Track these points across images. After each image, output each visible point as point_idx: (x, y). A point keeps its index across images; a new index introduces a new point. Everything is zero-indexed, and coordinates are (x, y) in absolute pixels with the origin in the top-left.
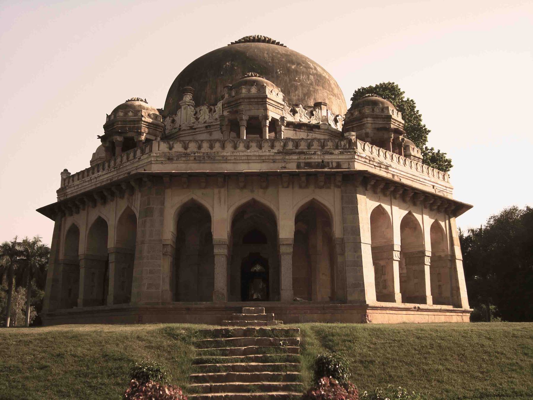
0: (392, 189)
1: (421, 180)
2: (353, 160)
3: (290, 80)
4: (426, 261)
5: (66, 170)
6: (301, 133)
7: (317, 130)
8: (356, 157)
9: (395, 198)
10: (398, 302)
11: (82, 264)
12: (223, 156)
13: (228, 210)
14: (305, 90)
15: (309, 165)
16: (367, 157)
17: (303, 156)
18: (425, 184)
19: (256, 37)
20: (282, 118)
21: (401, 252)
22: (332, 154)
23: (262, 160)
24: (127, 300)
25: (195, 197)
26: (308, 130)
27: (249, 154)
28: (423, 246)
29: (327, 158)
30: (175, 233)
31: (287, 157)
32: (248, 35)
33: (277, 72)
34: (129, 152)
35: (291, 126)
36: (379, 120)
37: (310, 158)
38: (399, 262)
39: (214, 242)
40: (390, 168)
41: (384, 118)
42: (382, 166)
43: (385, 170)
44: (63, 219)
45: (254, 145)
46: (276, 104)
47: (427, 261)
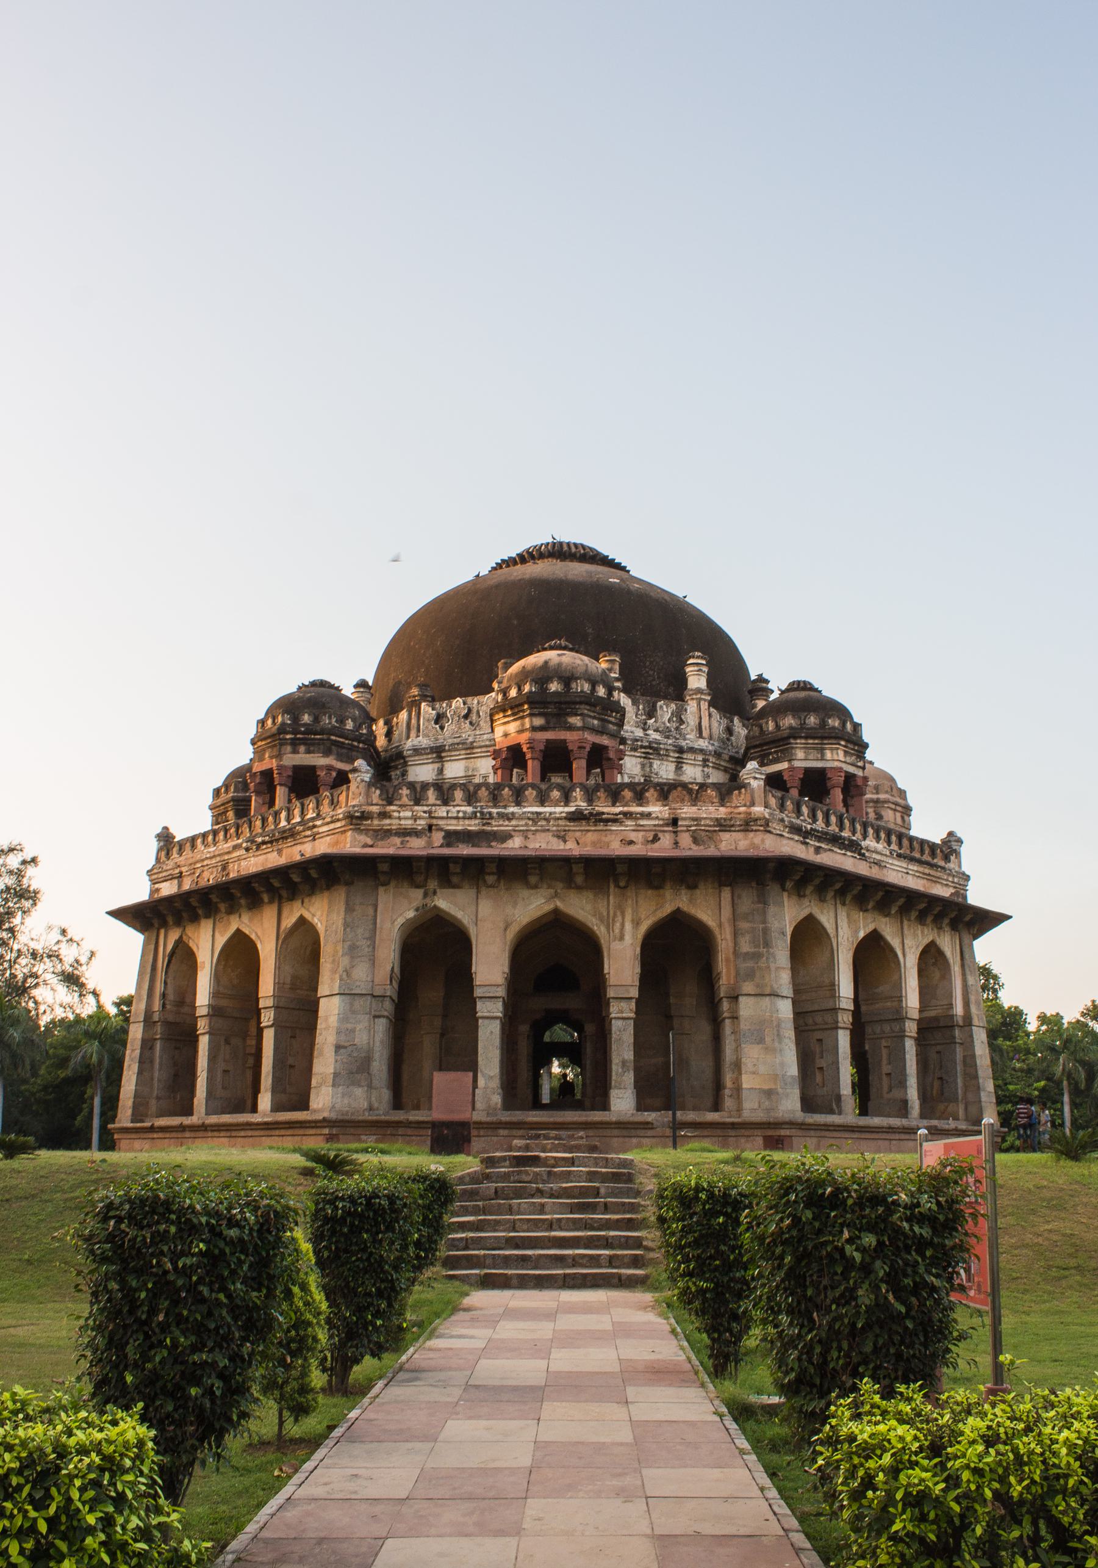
0: (838, 886)
4: (907, 1029)
5: (166, 828)
9: (844, 904)
10: (849, 1115)
11: (202, 1025)
13: (505, 930)
19: (565, 548)
21: (856, 1013)
24: (304, 1105)
28: (900, 999)
30: (397, 970)
34: (307, 801)
38: (851, 1031)
39: (478, 992)
44: (162, 931)
45: (556, 794)
47: (911, 1028)
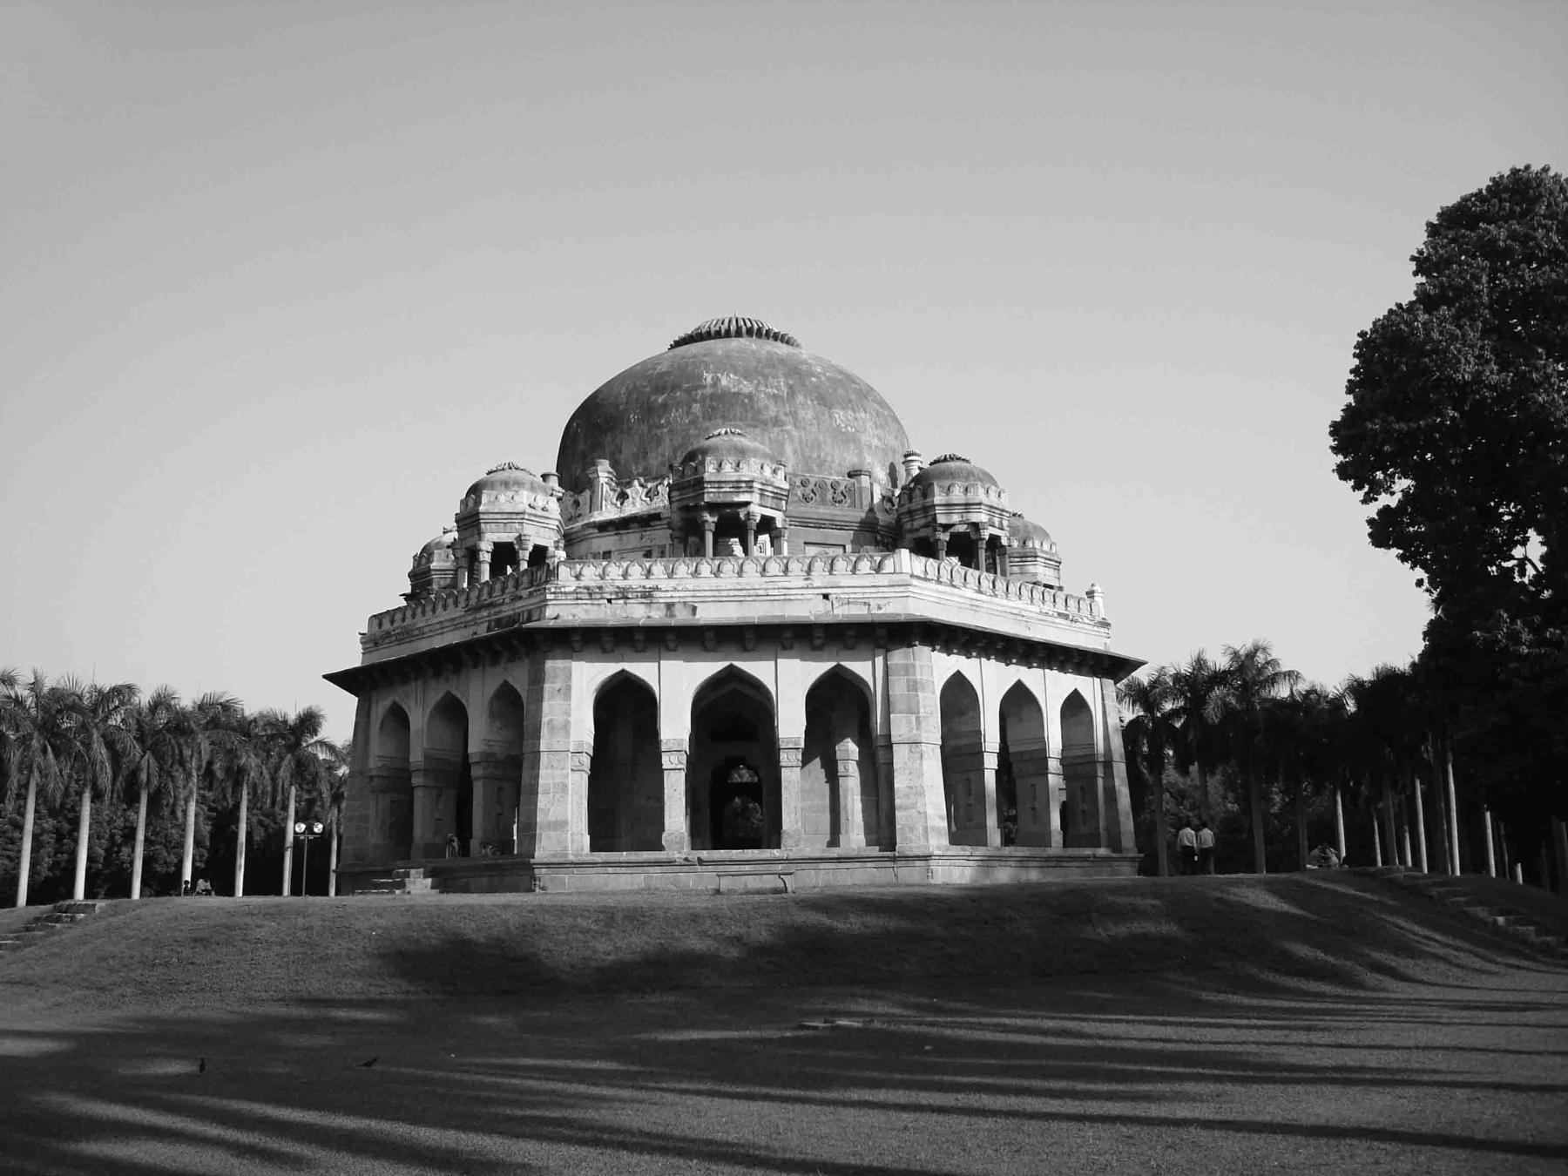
1: (770, 592)
2: (544, 604)
3: (650, 429)
6: (631, 535)
7: (658, 523)
8: (548, 597)
12: (419, 629)
14: (678, 440)
15: (499, 622)
16: (579, 590)
17: (493, 611)
18: (788, 597)
20: (519, 539)
22: (521, 598)
23: (455, 625)
25: (397, 699)
26: (642, 527)
27: (442, 619)
29: (519, 604)
31: (478, 616)
32: (727, 317)
33: (629, 420)
35: (609, 528)
36: (687, 490)
37: (500, 612)
40: (656, 594)
41: (694, 485)
42: (630, 596)
43: (643, 600)
46: (505, 516)
